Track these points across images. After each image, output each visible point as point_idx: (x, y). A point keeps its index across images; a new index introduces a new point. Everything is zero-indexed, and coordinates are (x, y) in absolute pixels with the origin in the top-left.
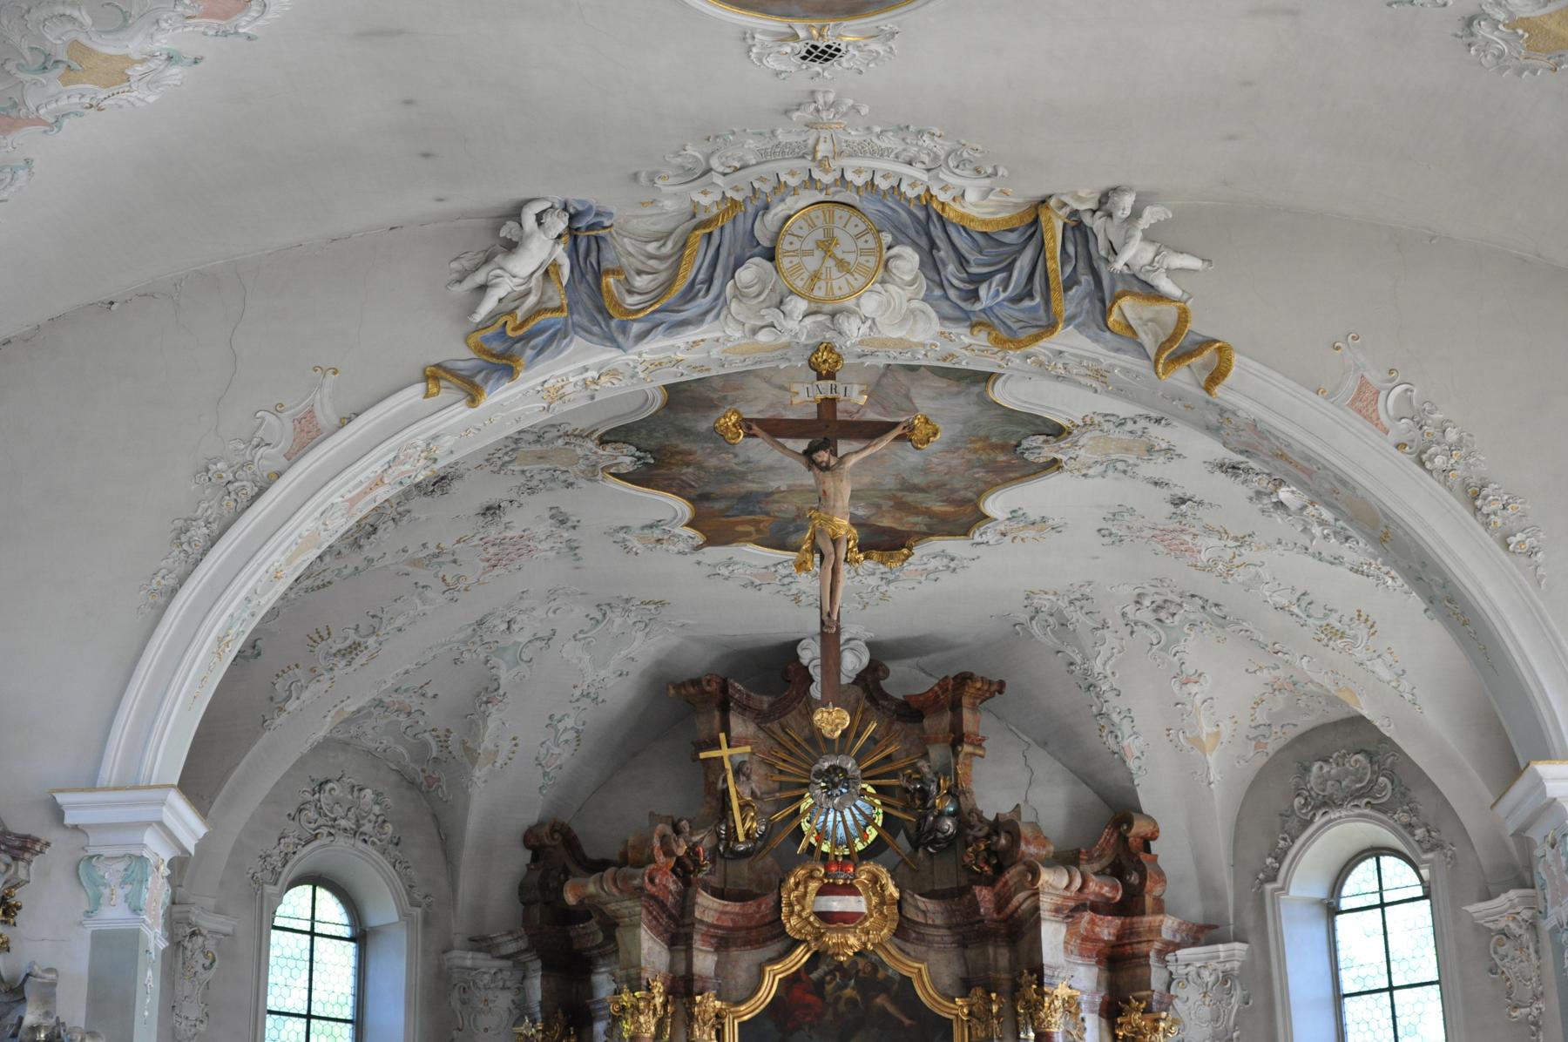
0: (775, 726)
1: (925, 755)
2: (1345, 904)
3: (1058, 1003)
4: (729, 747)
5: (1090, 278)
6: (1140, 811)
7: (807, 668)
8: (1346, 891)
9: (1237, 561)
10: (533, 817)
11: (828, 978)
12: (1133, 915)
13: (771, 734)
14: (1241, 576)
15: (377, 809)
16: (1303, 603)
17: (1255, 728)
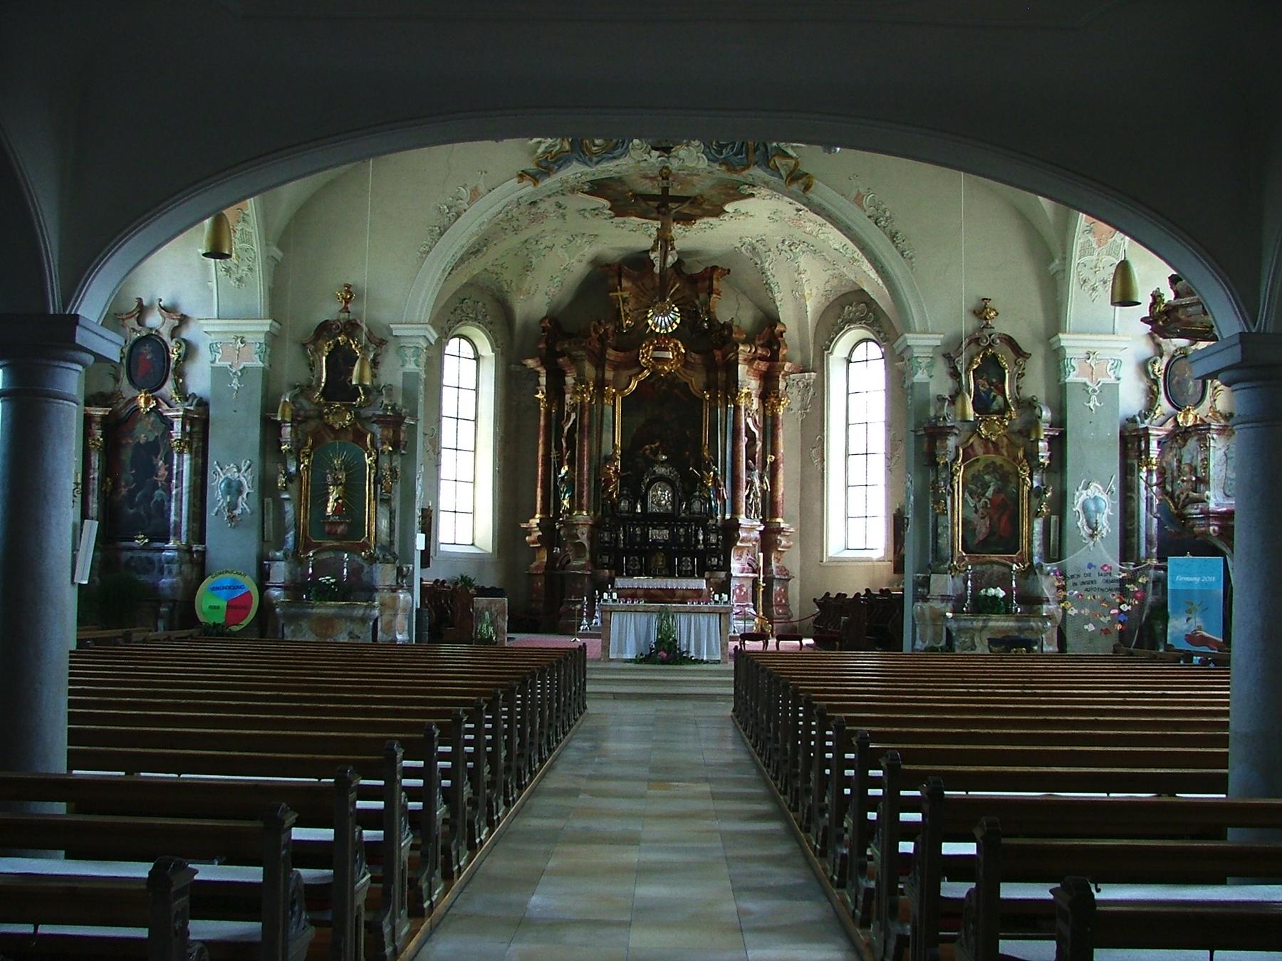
5: (764, 149)
16: (845, 248)
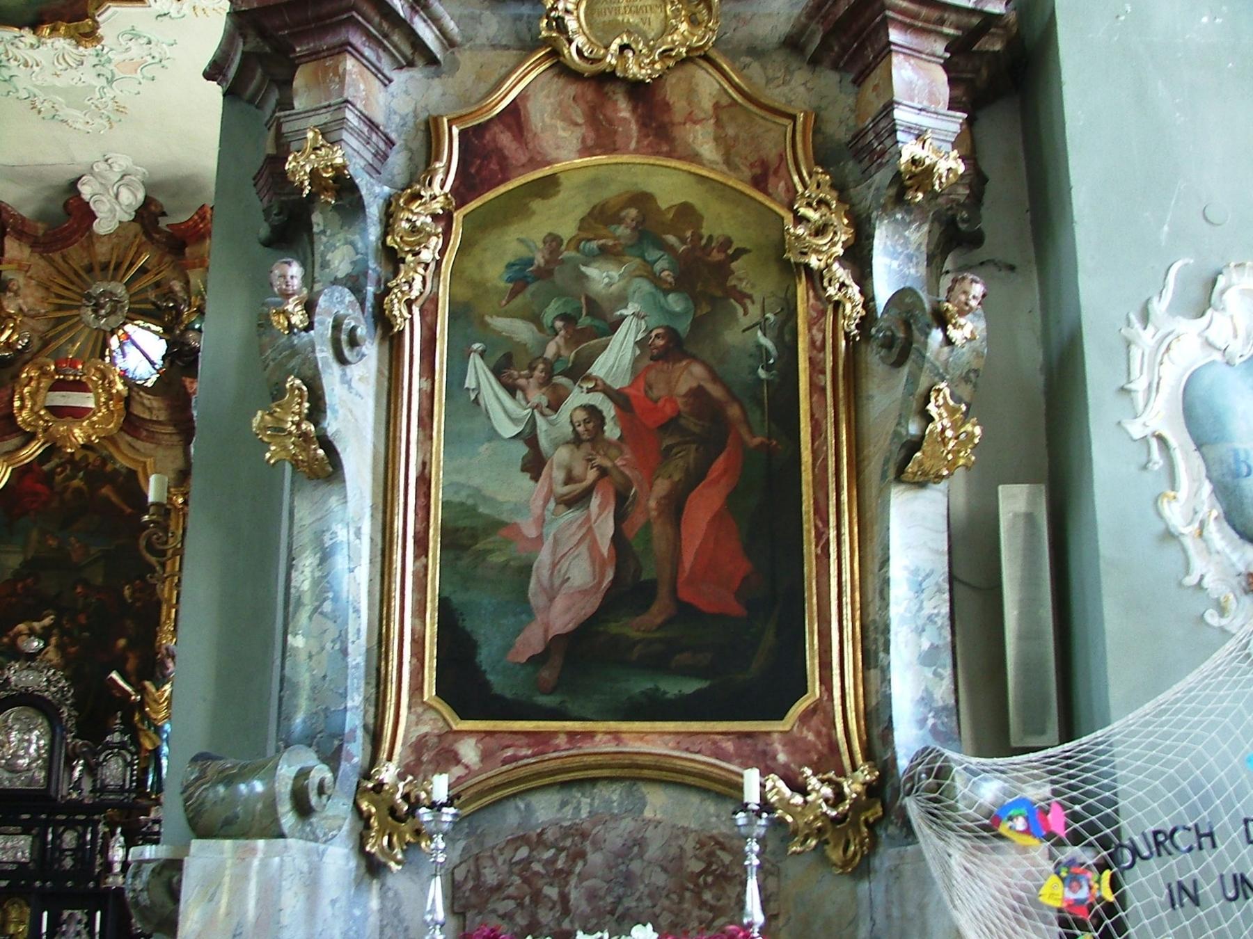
0: (57, 257)
7: (88, 203)
11: (59, 470)
13: (51, 262)
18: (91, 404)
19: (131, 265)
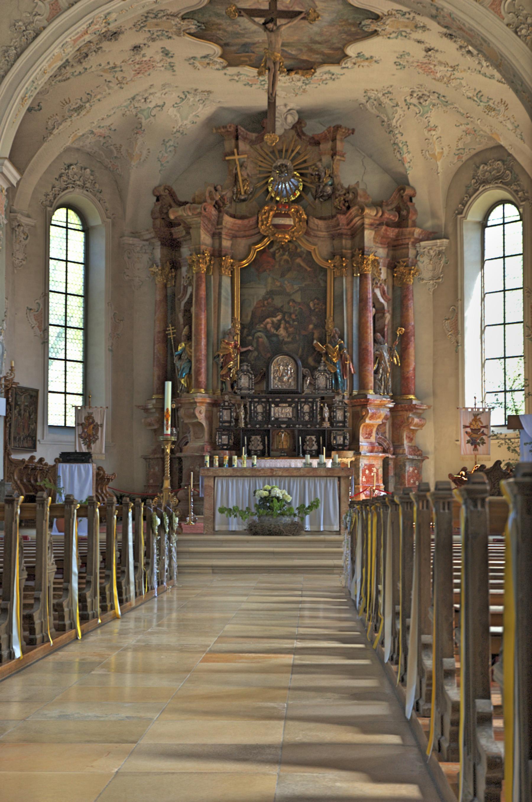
0: (258, 147)
1: (320, 160)
2: (489, 224)
3: (369, 262)
4: (238, 154)
6: (408, 184)
8: (490, 218)
9: (452, 77)
10: (156, 183)
12: (404, 227)
13: (256, 150)
14: (454, 83)
15: (92, 177)
17: (459, 150)
18: (292, 223)
19: (293, 151)
